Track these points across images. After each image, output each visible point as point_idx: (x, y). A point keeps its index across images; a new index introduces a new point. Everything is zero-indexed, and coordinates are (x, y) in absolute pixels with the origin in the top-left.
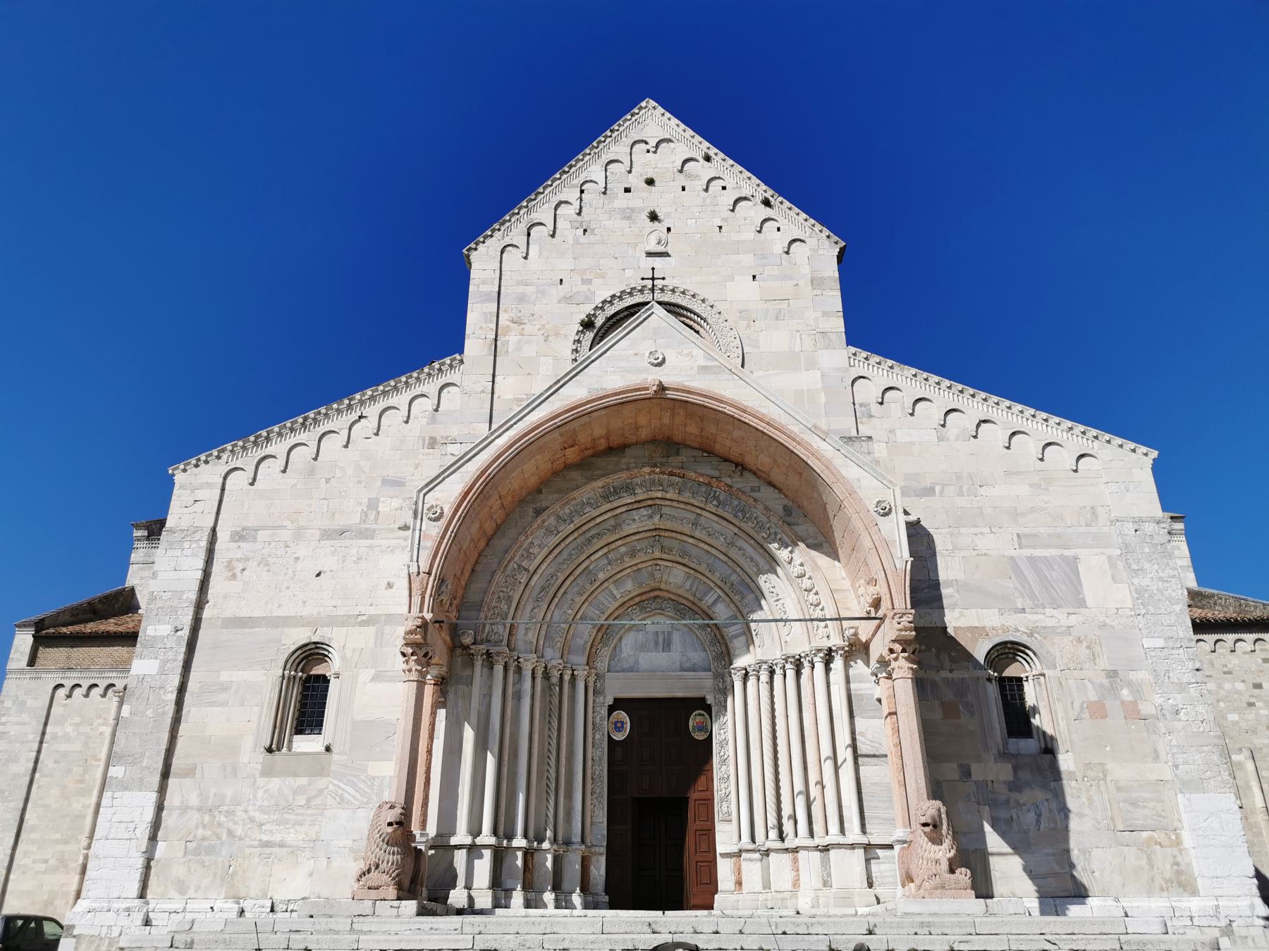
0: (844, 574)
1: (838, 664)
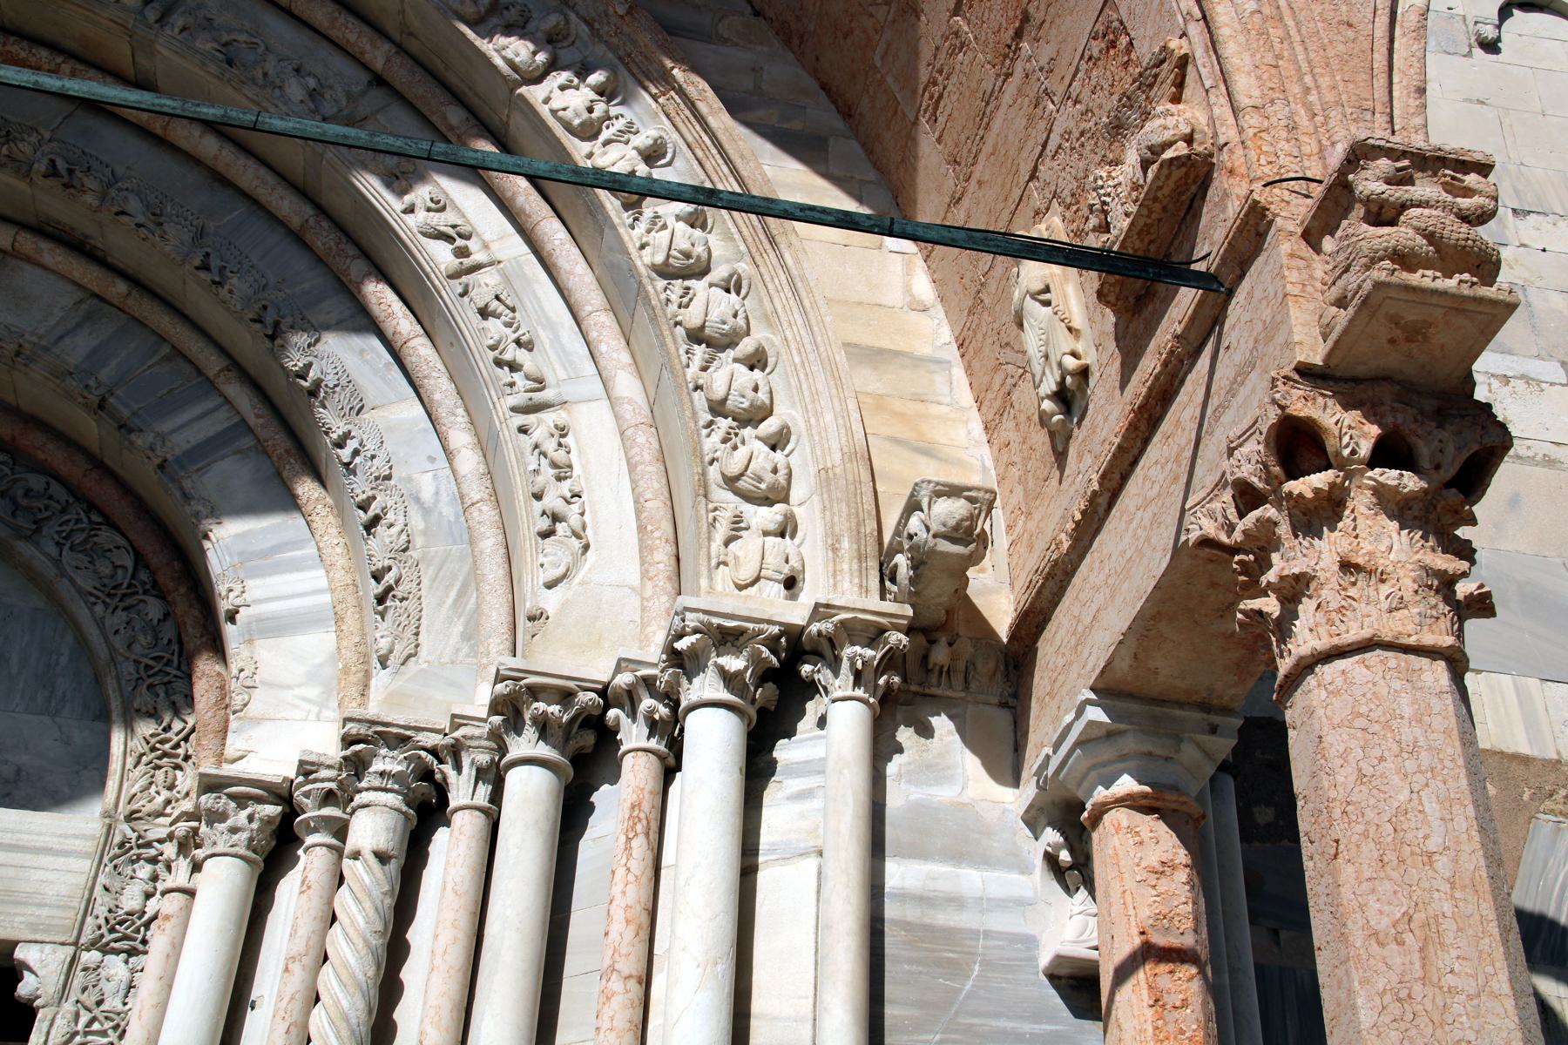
0: (923, 286)
1: (835, 727)
